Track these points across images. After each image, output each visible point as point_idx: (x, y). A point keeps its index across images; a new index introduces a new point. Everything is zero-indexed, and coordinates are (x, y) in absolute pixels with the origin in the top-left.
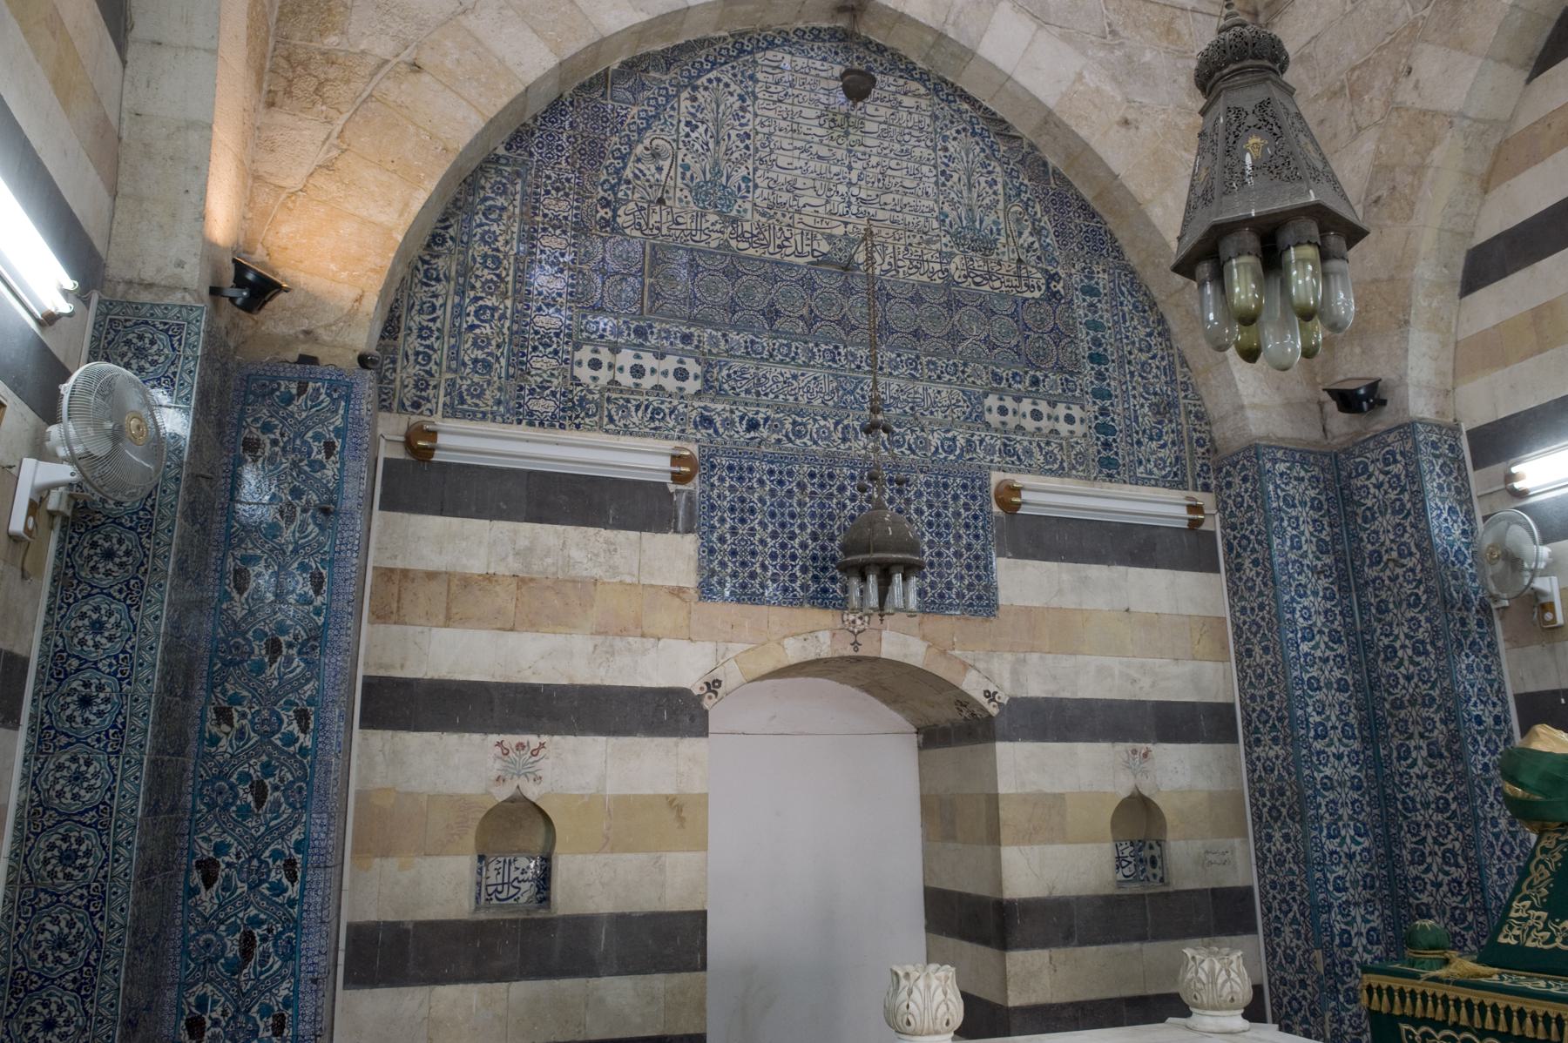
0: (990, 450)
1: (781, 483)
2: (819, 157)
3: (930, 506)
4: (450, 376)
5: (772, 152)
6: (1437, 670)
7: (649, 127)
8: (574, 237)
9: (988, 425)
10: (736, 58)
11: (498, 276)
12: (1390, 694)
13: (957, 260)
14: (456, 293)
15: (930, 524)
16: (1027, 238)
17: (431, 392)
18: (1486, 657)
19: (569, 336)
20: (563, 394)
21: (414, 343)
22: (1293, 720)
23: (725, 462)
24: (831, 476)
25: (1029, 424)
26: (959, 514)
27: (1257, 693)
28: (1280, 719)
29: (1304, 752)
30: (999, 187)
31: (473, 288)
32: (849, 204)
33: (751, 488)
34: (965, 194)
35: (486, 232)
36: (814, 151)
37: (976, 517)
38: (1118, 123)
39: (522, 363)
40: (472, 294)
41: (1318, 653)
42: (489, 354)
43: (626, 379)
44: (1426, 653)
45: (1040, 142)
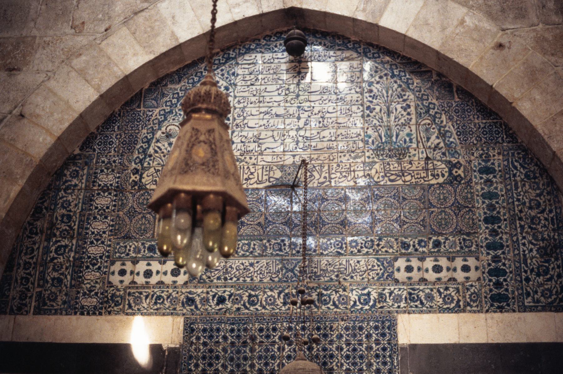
0: (397, 299)
1: (238, 337)
2: (277, 116)
3: (348, 344)
4: (39, 290)
5: (245, 118)
7: (166, 119)
8: (116, 196)
9: (397, 281)
10: (224, 64)
11: (70, 226)
13: (377, 166)
14: (46, 240)
15: (348, 357)
16: (434, 140)
17: (28, 300)
19: (108, 257)
20: (102, 294)
21: (21, 272)
23: (201, 327)
24: (274, 329)
25: (431, 276)
26: (371, 348)
30: (412, 109)
31: (55, 235)
32: (297, 142)
33: (218, 342)
34: (385, 119)
35: (64, 201)
36: (273, 112)
37: (384, 349)
38: (493, 48)
39: (80, 277)
40: (54, 239)
42: (61, 274)
43: (141, 280)
45: (444, 70)
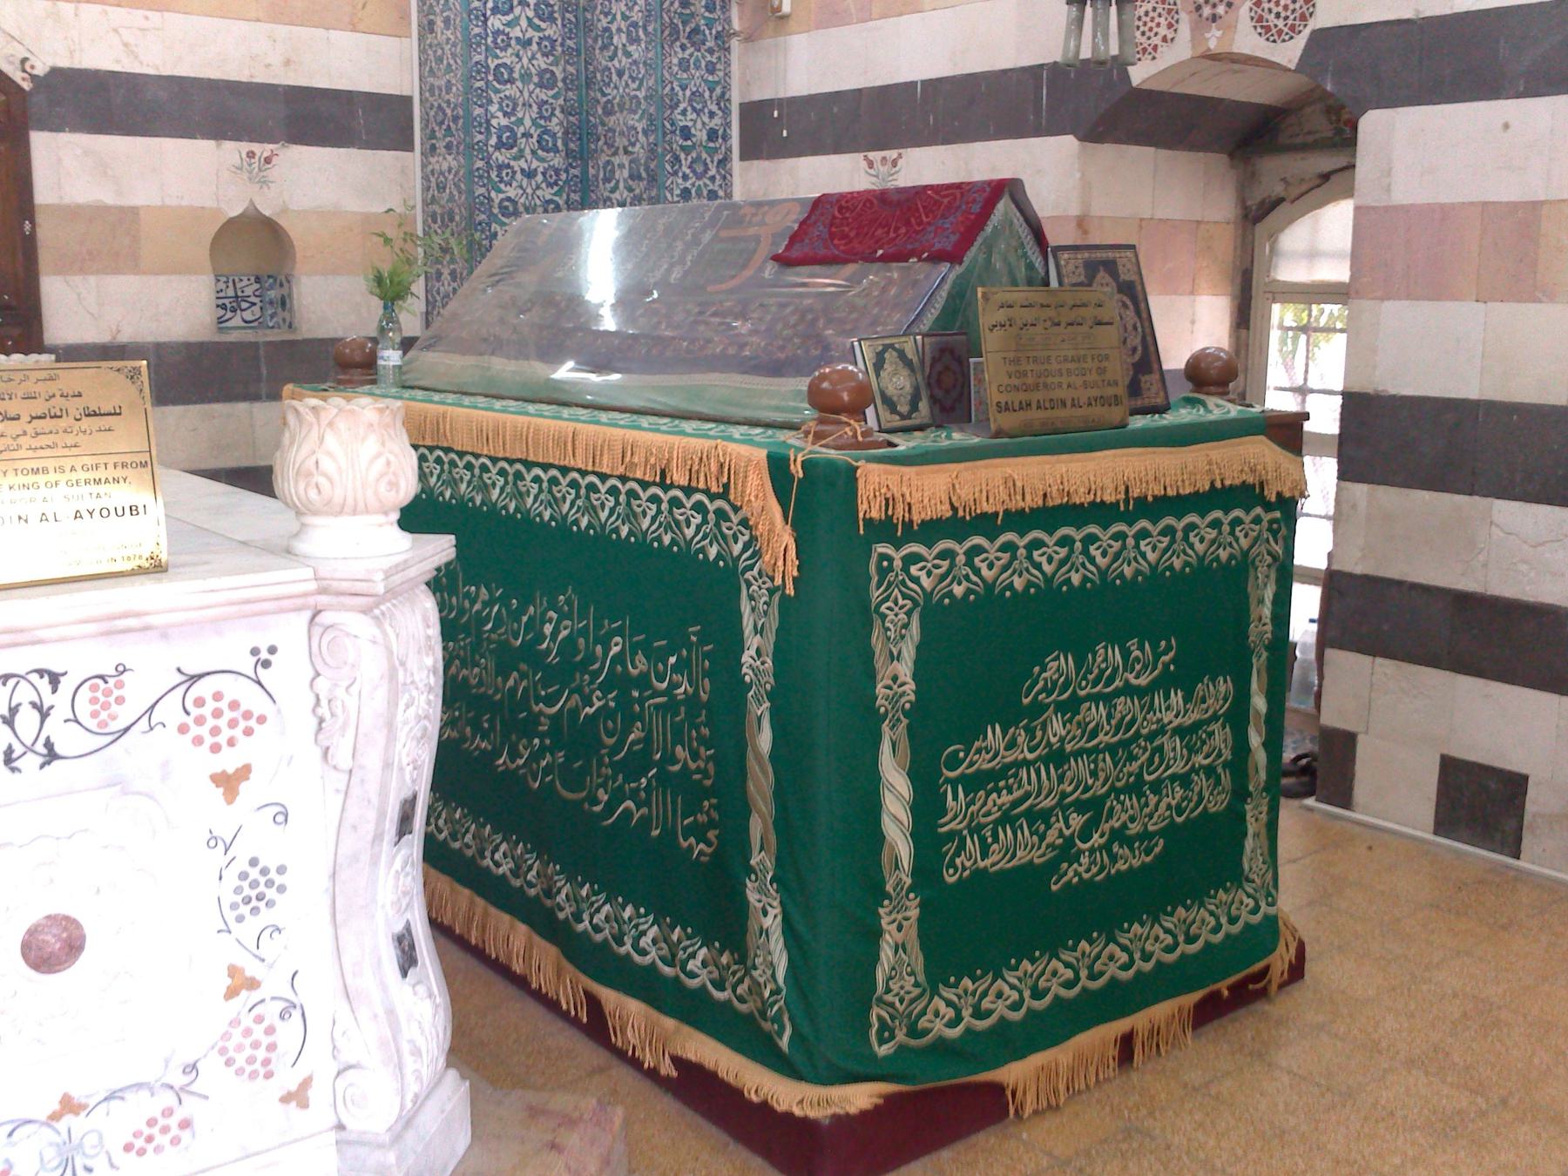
6: (645, 63)
12: (604, 95)
18: (711, 51)
22: (470, 121)
27: (437, 83)
28: (455, 119)
29: (480, 164)
41: (516, 32)
44: (637, 41)
